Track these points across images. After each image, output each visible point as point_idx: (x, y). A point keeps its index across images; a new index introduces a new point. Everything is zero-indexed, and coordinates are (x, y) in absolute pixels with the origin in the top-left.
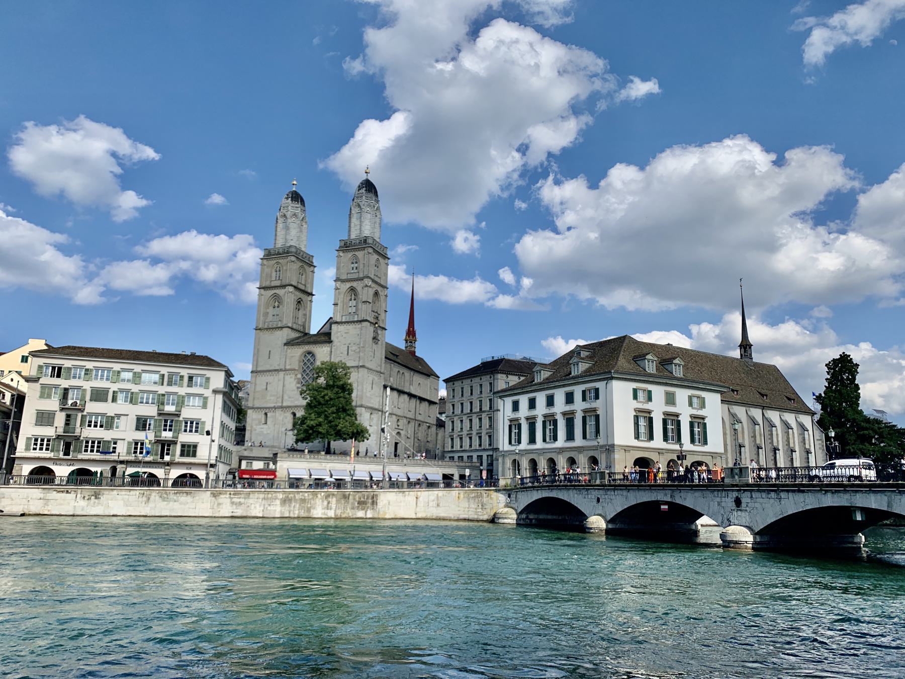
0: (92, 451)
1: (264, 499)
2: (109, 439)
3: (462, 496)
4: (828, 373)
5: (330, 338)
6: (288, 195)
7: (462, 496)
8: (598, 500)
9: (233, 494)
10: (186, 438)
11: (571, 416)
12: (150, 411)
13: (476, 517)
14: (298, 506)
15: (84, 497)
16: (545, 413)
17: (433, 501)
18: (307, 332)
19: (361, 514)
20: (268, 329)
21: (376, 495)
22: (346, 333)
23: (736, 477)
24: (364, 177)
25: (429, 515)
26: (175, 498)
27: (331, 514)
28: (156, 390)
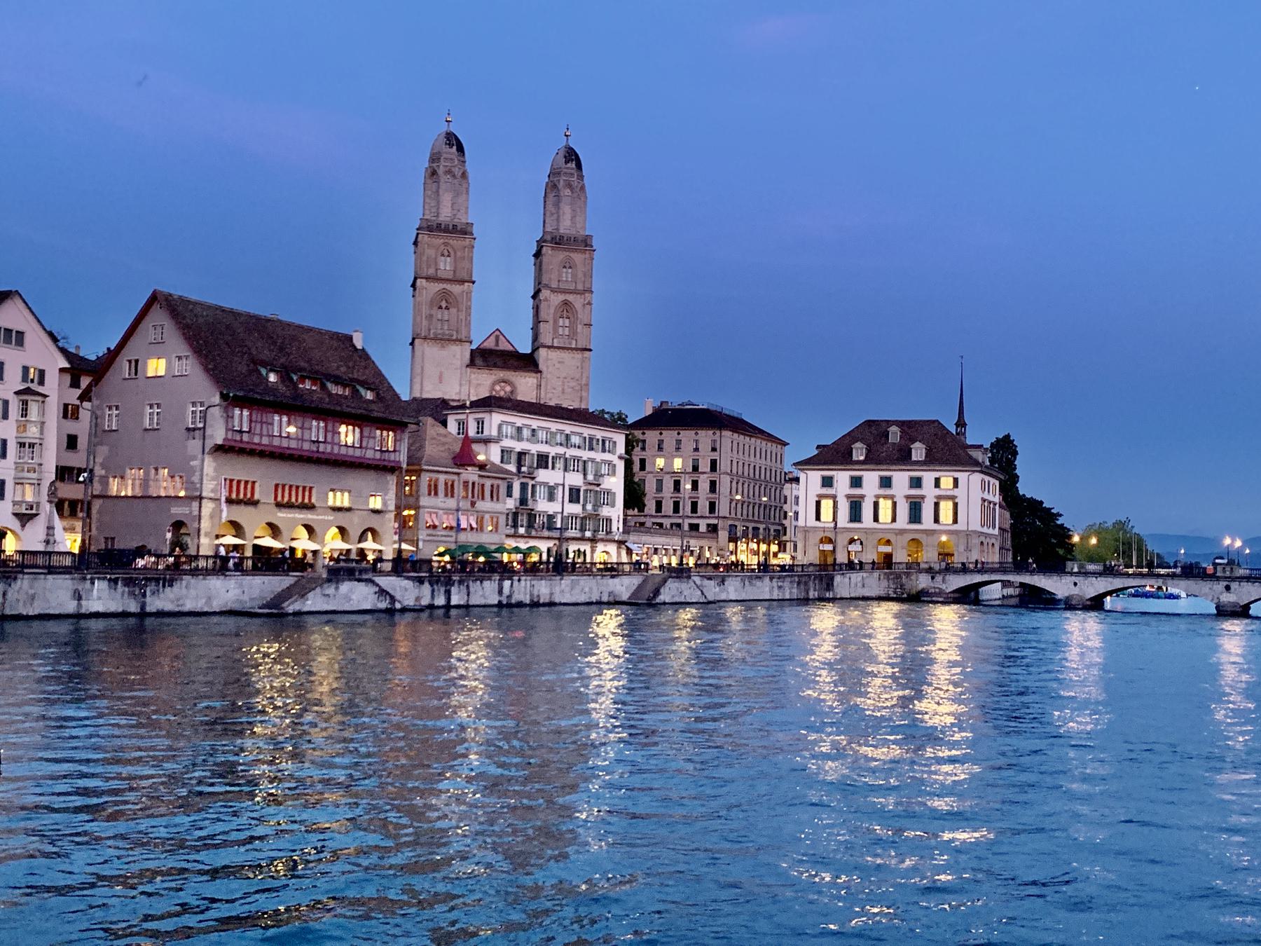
6: (448, 139)
8: (1075, 584)
11: (918, 500)
20: (435, 339)
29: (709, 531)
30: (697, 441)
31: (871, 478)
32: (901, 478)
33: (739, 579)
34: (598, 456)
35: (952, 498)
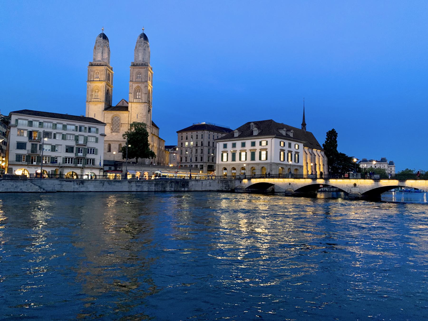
0: (69, 163)
1: (148, 184)
2: (54, 156)
3: (220, 182)
4: (327, 136)
5: (128, 110)
6: (100, 35)
7: (220, 182)
9: (137, 182)
10: (89, 156)
12: (72, 143)
13: (225, 190)
14: (161, 186)
15: (77, 184)
16: (241, 149)
17: (208, 184)
18: (111, 105)
19: (183, 189)
21: (188, 182)
22: (136, 108)
23: (355, 177)
24: (142, 32)
25: (207, 190)
26: (114, 184)
27: (173, 189)
28: (75, 134)
30: (197, 135)
31: (239, 143)
32: (248, 143)
33: (99, 181)
35: (266, 149)
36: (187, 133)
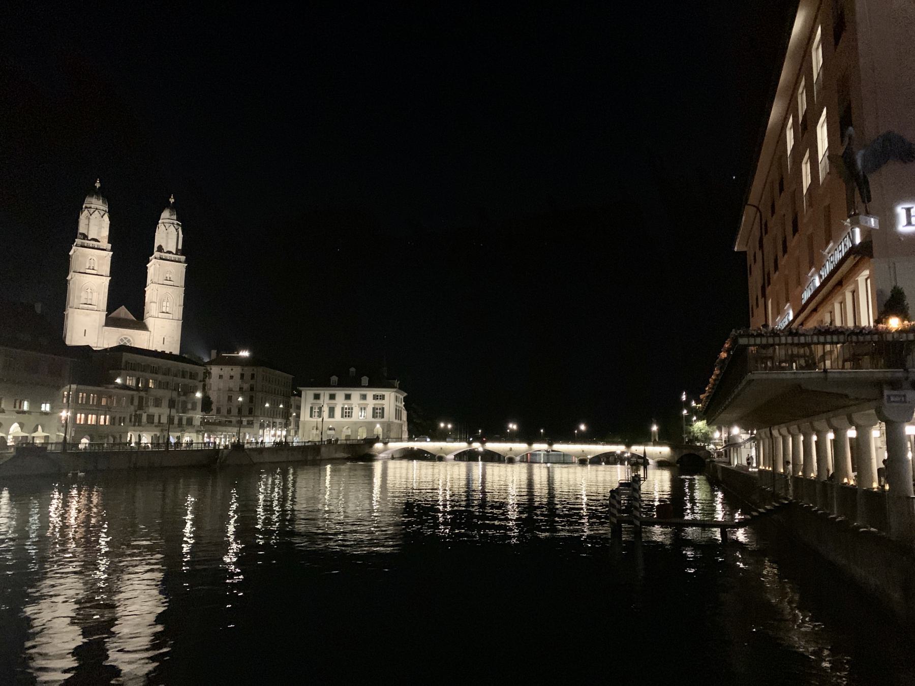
22: (162, 327)
29: (248, 424)
34: (187, 381)
36: (221, 369)
